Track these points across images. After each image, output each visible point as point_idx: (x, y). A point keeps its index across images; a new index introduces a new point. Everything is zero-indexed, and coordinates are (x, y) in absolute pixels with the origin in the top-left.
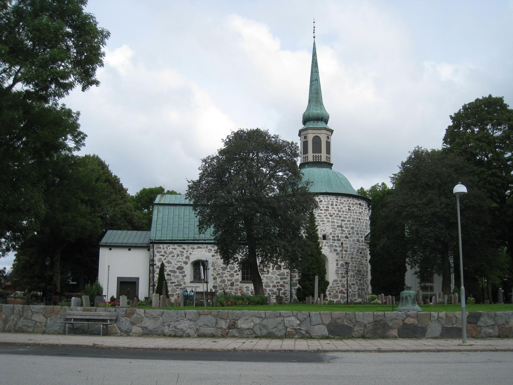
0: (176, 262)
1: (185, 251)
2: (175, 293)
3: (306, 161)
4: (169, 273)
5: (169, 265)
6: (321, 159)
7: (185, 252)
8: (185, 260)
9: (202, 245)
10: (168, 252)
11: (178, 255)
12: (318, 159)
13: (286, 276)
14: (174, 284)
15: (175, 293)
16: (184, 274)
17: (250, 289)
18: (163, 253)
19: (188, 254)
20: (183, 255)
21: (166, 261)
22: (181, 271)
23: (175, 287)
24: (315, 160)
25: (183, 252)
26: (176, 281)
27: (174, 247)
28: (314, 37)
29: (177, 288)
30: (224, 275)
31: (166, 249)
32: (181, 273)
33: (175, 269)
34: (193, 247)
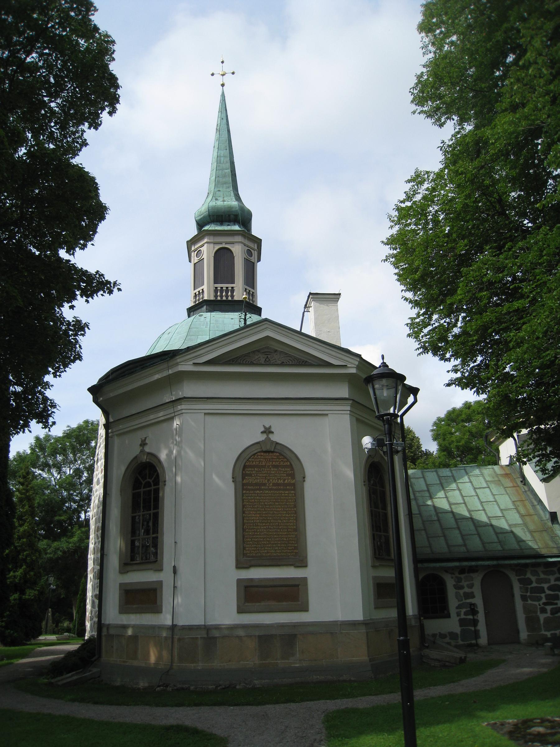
6: (232, 296)
12: (227, 296)
24: (219, 298)
28: (223, 85)
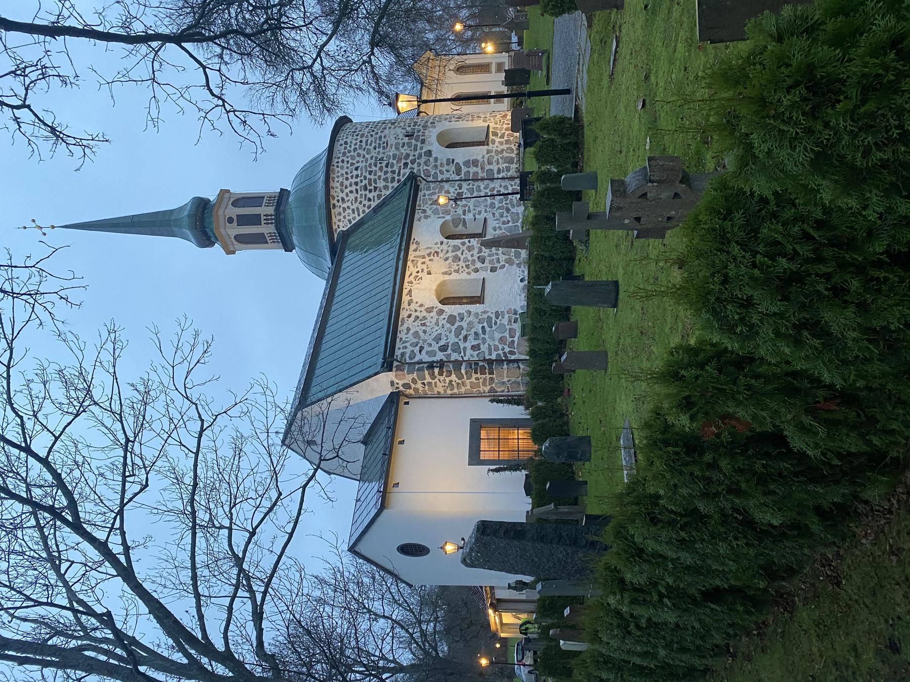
0: (437, 328)
1: (414, 314)
2: (508, 327)
3: (273, 217)
4: (461, 337)
5: (443, 336)
7: (418, 314)
8: (434, 314)
9: (404, 290)
10: (415, 340)
11: (424, 325)
13: (475, 187)
14: (488, 329)
15: (508, 327)
16: (465, 314)
17: (497, 226)
18: (417, 349)
19: (423, 309)
20: (424, 317)
21: (434, 343)
22: (458, 318)
23: (494, 327)
25: (417, 317)
26: (481, 326)
27: (405, 331)
29: (496, 323)
30: (470, 258)
31: (408, 345)
32: (462, 319)
33: (453, 328)
34: (406, 303)
